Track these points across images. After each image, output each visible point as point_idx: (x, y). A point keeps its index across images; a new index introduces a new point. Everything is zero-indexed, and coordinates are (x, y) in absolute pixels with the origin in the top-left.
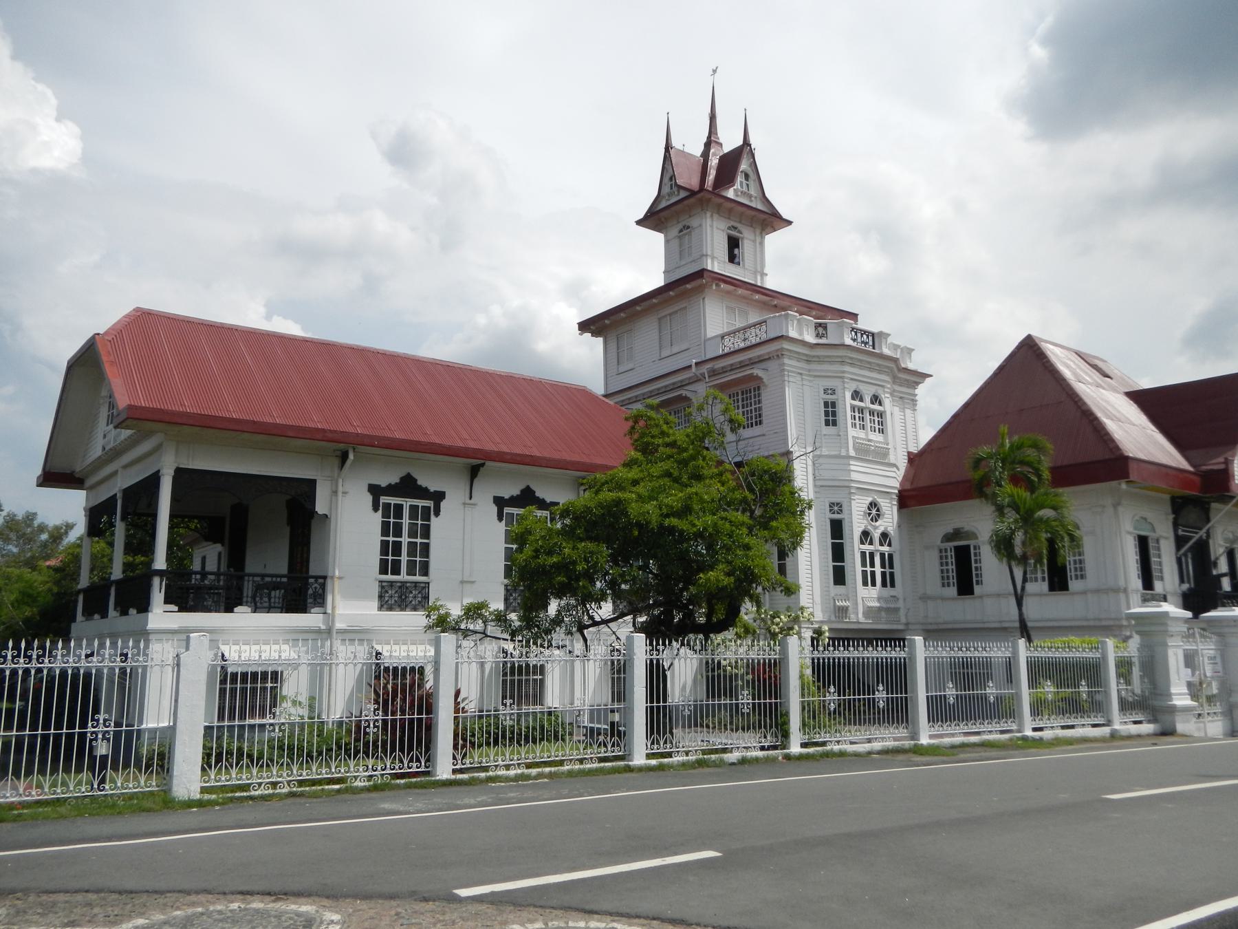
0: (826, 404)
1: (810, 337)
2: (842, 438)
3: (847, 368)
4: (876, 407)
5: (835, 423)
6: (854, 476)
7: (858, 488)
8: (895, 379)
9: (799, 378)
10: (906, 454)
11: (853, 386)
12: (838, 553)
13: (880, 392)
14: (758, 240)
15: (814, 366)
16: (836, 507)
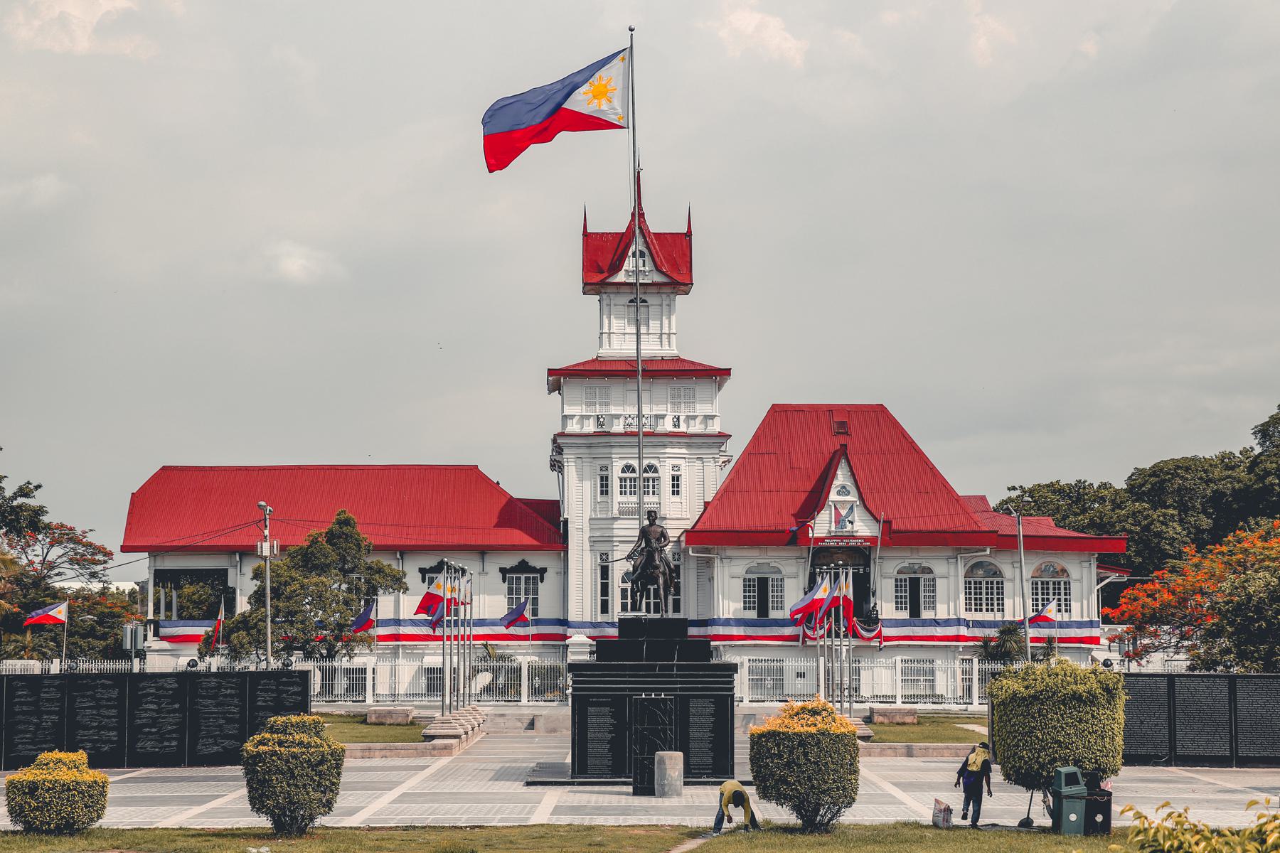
0: (602, 478)
1: (590, 427)
2: (607, 506)
3: (614, 450)
4: (651, 475)
5: (607, 494)
6: (616, 532)
7: (619, 541)
8: (689, 446)
9: (579, 461)
10: (703, 504)
11: (625, 462)
12: (605, 590)
13: (654, 462)
14: (665, 303)
15: (594, 451)
16: (604, 556)
